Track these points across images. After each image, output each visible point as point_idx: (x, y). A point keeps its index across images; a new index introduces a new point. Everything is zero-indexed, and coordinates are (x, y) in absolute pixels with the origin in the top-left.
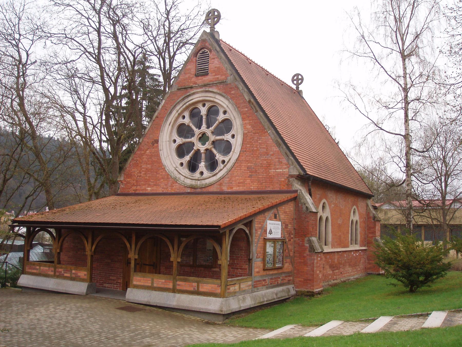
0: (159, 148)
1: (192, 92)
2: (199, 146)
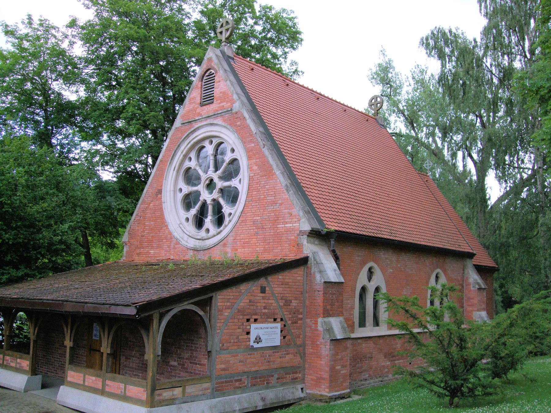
0: (163, 200)
1: (196, 126)
2: (206, 196)
